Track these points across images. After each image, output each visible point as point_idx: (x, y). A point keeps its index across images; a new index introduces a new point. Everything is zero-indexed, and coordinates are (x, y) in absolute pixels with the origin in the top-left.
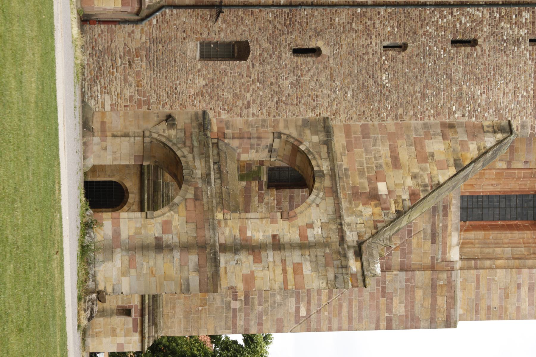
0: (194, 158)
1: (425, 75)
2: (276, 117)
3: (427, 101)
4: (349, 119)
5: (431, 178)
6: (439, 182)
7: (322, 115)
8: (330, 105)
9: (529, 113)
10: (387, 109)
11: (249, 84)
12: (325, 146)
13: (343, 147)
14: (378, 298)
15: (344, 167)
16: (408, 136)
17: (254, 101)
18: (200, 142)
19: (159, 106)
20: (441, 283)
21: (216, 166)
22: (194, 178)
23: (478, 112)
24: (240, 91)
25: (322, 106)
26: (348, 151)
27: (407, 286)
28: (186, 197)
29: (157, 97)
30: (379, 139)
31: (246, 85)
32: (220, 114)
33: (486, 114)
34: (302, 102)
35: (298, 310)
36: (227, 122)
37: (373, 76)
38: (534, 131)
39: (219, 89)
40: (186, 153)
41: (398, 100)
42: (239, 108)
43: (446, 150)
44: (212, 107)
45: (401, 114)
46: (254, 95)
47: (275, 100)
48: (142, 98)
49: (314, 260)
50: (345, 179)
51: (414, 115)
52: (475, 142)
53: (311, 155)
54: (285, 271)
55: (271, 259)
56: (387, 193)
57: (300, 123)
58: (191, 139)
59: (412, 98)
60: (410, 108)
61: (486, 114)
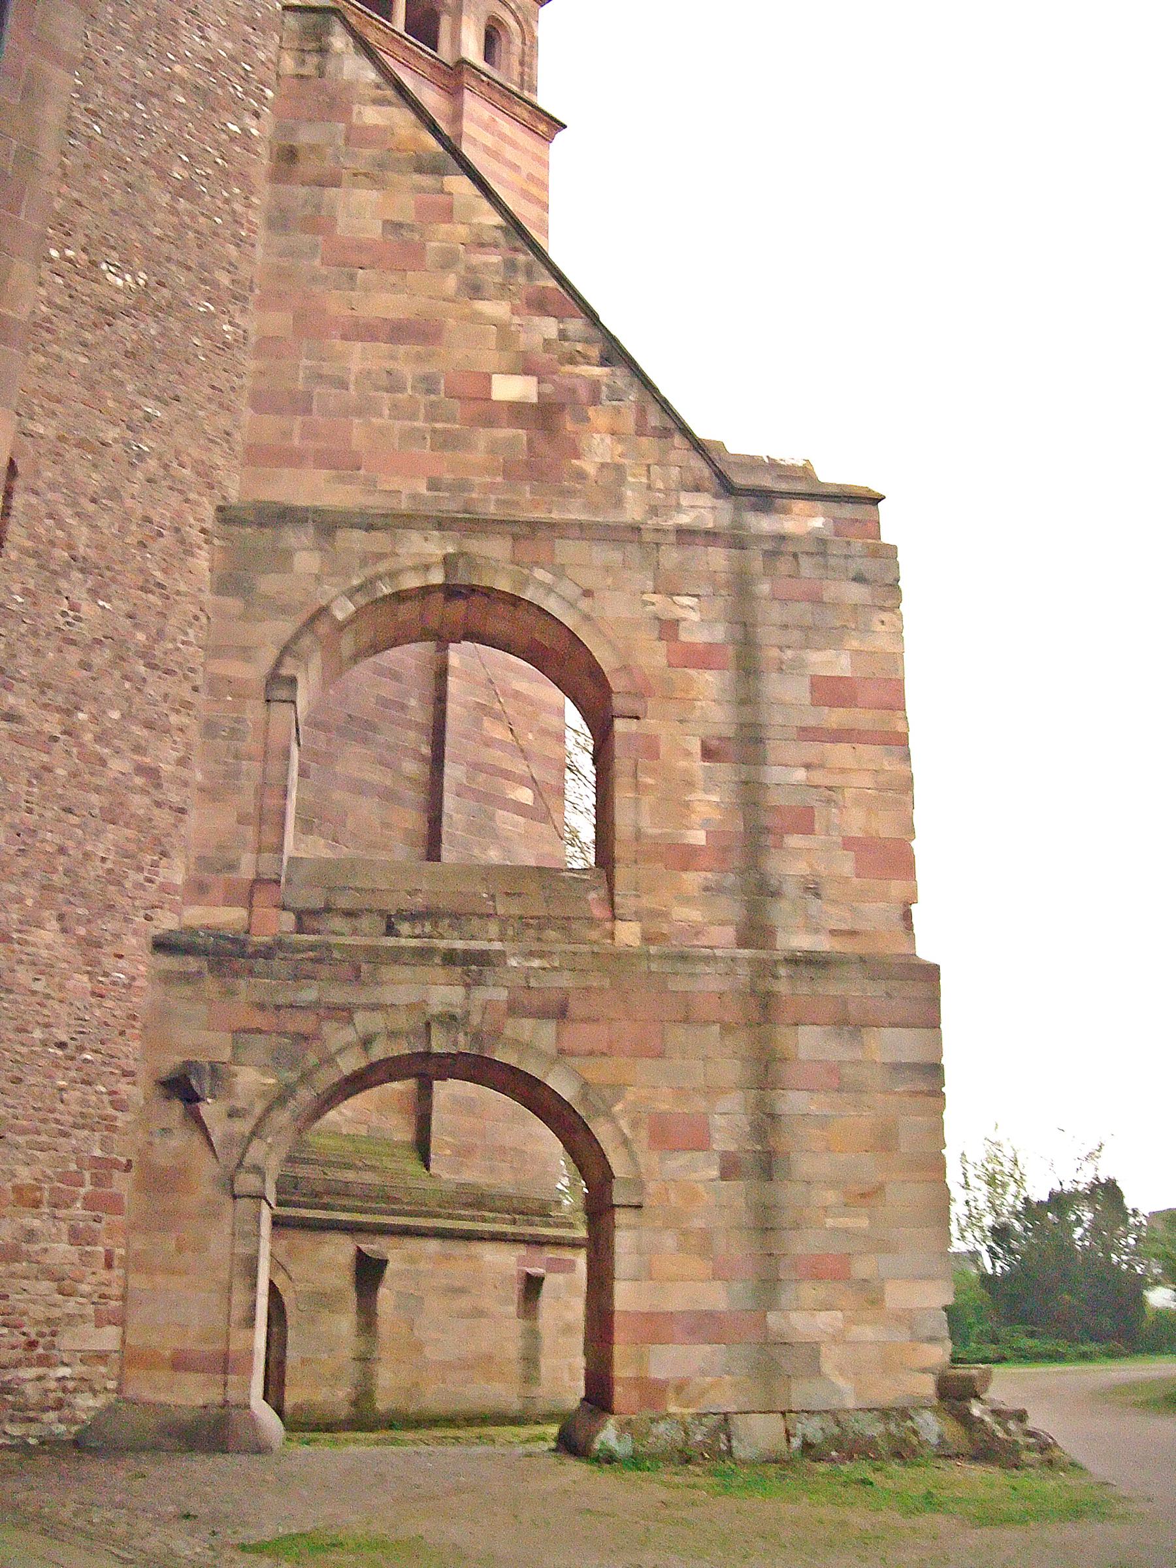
1: (128, 159)
2: (199, 683)
4: (228, 442)
5: (482, 245)
10: (214, 316)
11: (75, 750)
12: (340, 534)
13: (341, 480)
15: (423, 490)
16: (314, 279)
17: (138, 749)
18: (299, 976)
19: (119, 1124)
21: (405, 928)
24: (98, 790)
25: (179, 515)
26: (359, 469)
28: (553, 1051)
29: (83, 1127)
31: (82, 765)
32: (165, 888)
35: (519, 808)
37: (108, 314)
39: (82, 872)
40: (348, 1035)
41: (189, 269)
42: (156, 811)
44: (142, 913)
46: (116, 742)
47: (142, 669)
48: (82, 1191)
50: (474, 495)
51: (238, 245)
53: (379, 584)
55: (800, 775)
57: (233, 604)
59: (189, 228)
60: (218, 246)
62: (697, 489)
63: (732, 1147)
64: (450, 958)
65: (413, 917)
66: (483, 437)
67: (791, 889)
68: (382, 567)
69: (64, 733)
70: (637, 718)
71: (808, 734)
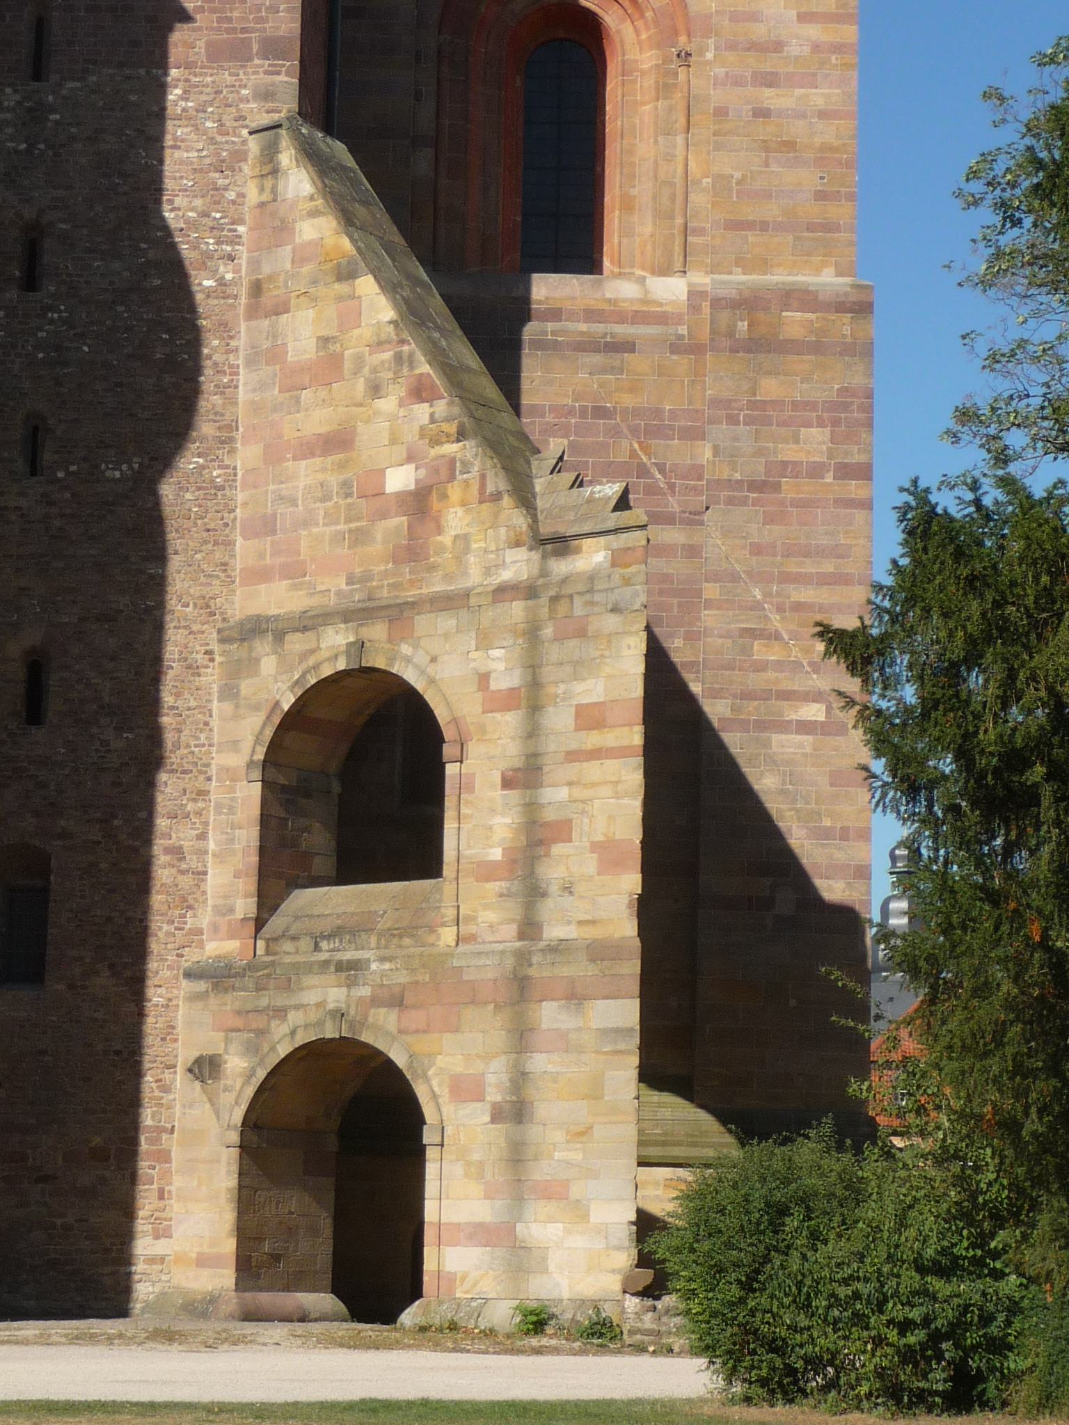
0: (297, 1007)
3: (186, 357)
5: (380, 343)
6: (390, 322)
7: (210, 647)
8: (183, 623)
9: (229, 79)
10: (203, 467)
11: (114, 847)
12: (288, 638)
13: (295, 587)
14: (782, 503)
15: (344, 587)
18: (259, 988)
20: (743, 326)
21: (324, 945)
22: (348, 1006)
23: (221, 218)
26: (305, 576)
27: (749, 421)
30: (280, 490)
33: (231, 195)
36: (218, 910)
38: (284, 66)
40: (284, 1029)
42: (180, 878)
43: (314, 304)
49: (568, 669)
50: (374, 584)
51: (223, 393)
52: (298, 225)
53: (309, 676)
54: (596, 754)
56: (411, 467)
58: (250, 1015)
61: (231, 195)
63: (499, 1098)
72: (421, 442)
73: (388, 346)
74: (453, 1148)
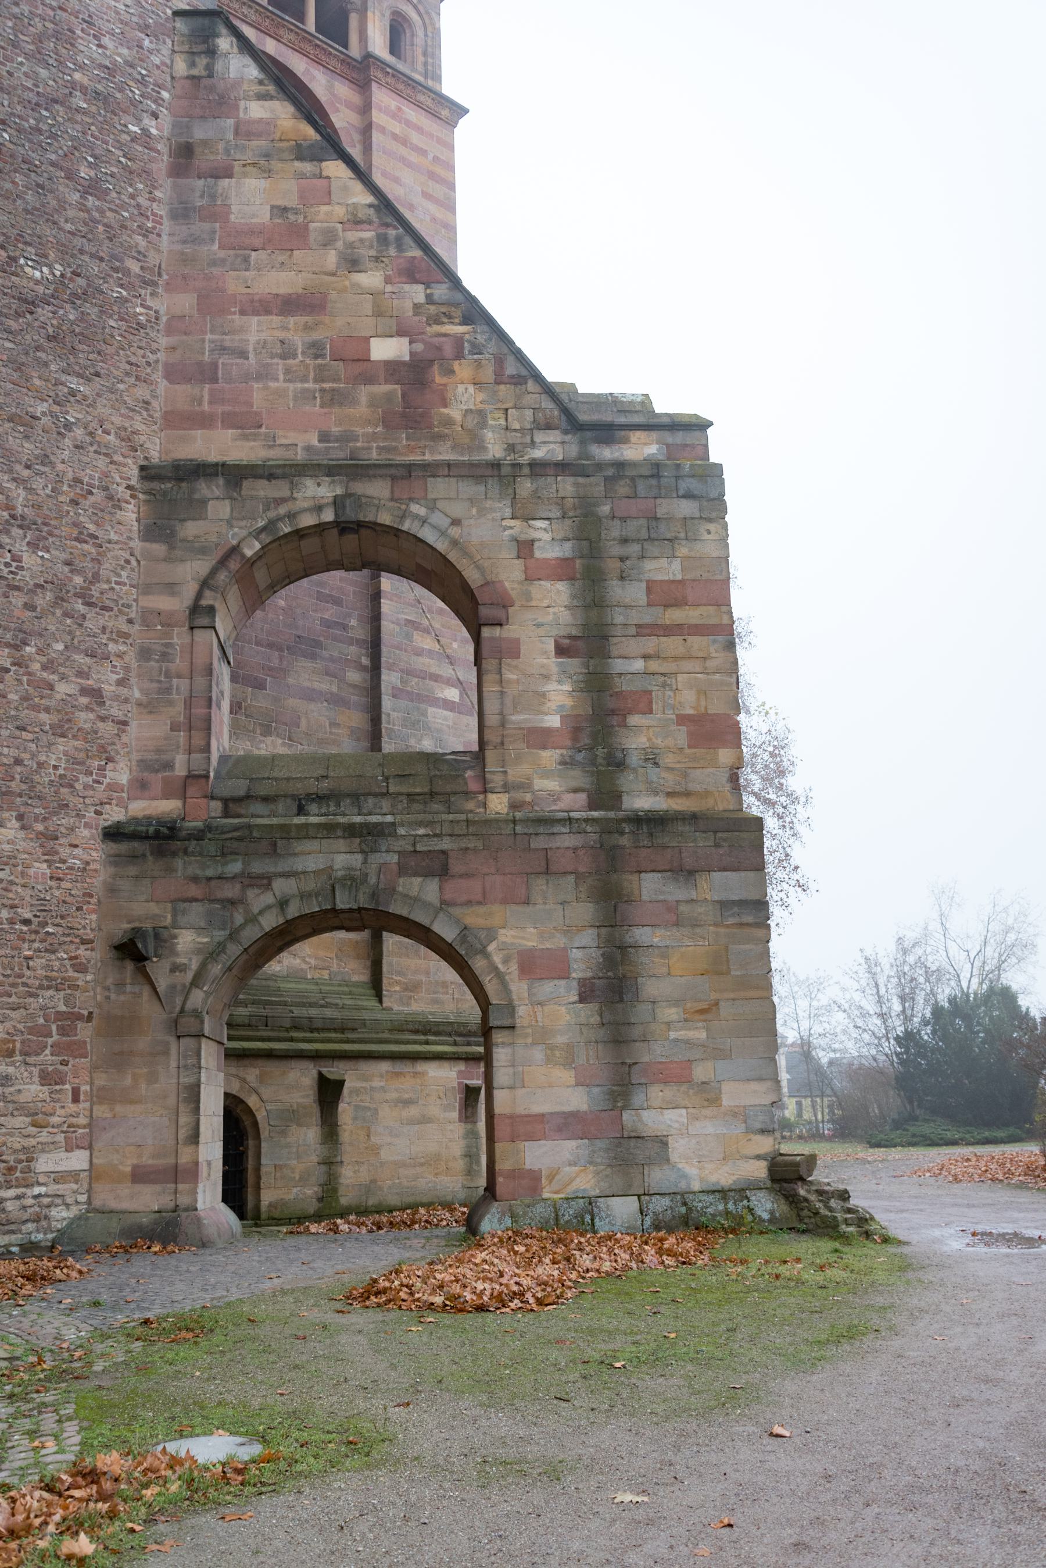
1: (37, 163)
2: (133, 615)
3: (111, 187)
4: (147, 410)
10: (127, 301)
11: (25, 678)
13: (245, 437)
15: (315, 442)
16: (214, 263)
17: (80, 674)
19: (80, 983)
21: (313, 808)
24: (47, 710)
25: (106, 475)
26: (260, 426)
28: (436, 902)
29: (49, 988)
30: (222, 341)
31: (31, 690)
32: (112, 787)
34: (92, 528)
37: (29, 304)
39: (37, 778)
40: (268, 899)
41: (101, 259)
42: (101, 725)
43: (266, 175)
44: (93, 809)
45: (142, 268)
46: (62, 670)
47: (80, 607)
48: (50, 1041)
50: (359, 444)
51: (144, 236)
52: (242, 104)
53: (281, 525)
55: (638, 665)
57: (159, 549)
58: (213, 883)
59: (98, 222)
60: (125, 237)
62: (548, 427)
64: (352, 831)
65: (320, 798)
66: (365, 392)
67: (634, 760)
68: (282, 510)
69: (14, 664)
70: (501, 625)
71: (643, 630)
72: (417, 318)
73: (366, 226)
74: (530, 1031)
